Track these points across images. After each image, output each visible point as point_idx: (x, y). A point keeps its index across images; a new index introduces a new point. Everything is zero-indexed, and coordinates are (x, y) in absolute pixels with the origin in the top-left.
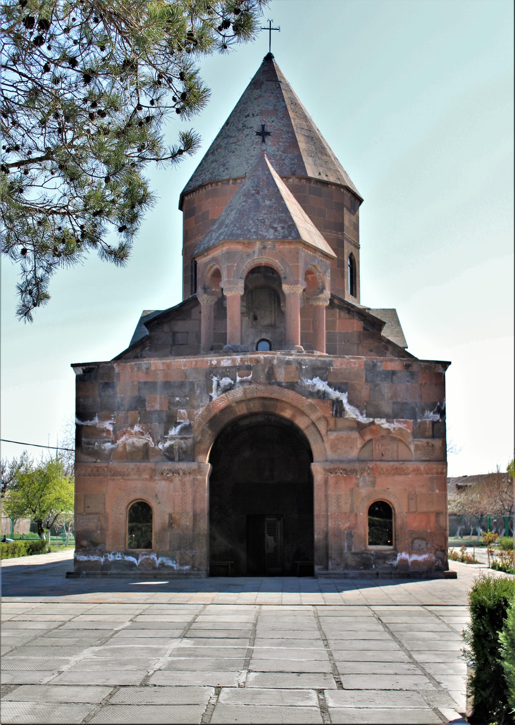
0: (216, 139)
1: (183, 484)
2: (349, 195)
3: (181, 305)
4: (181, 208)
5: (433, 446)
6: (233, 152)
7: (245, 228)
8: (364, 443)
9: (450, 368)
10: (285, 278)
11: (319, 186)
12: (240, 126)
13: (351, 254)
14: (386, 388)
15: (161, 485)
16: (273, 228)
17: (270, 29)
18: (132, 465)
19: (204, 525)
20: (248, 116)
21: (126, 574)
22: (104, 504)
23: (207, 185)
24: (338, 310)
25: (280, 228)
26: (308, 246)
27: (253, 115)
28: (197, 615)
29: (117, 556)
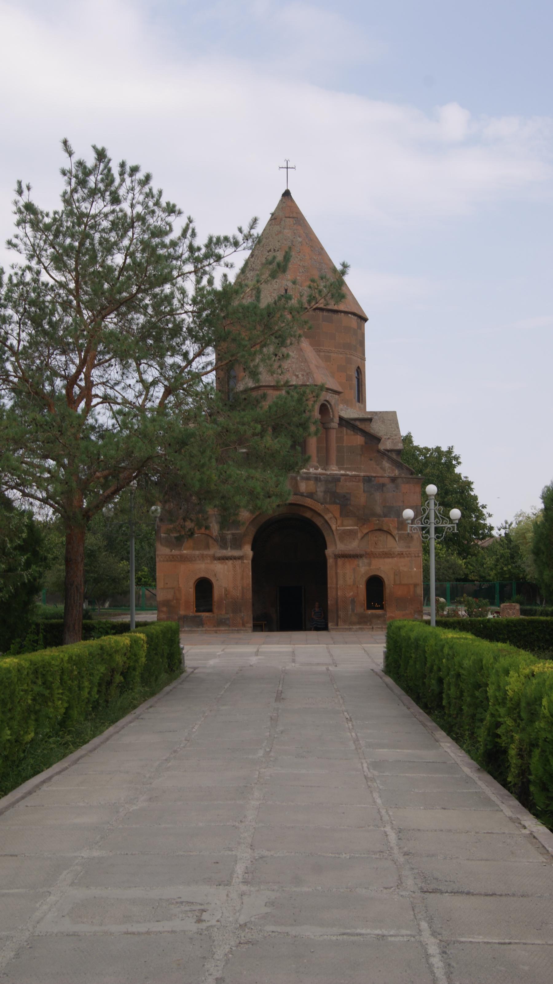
1: (234, 567)
2: (356, 318)
5: (412, 537)
8: (363, 535)
11: (330, 314)
13: (358, 367)
14: (378, 496)
15: (219, 567)
17: (287, 168)
18: (197, 552)
19: (249, 595)
20: (270, 251)
21: (195, 631)
22: (178, 581)
24: (345, 429)
27: (274, 250)
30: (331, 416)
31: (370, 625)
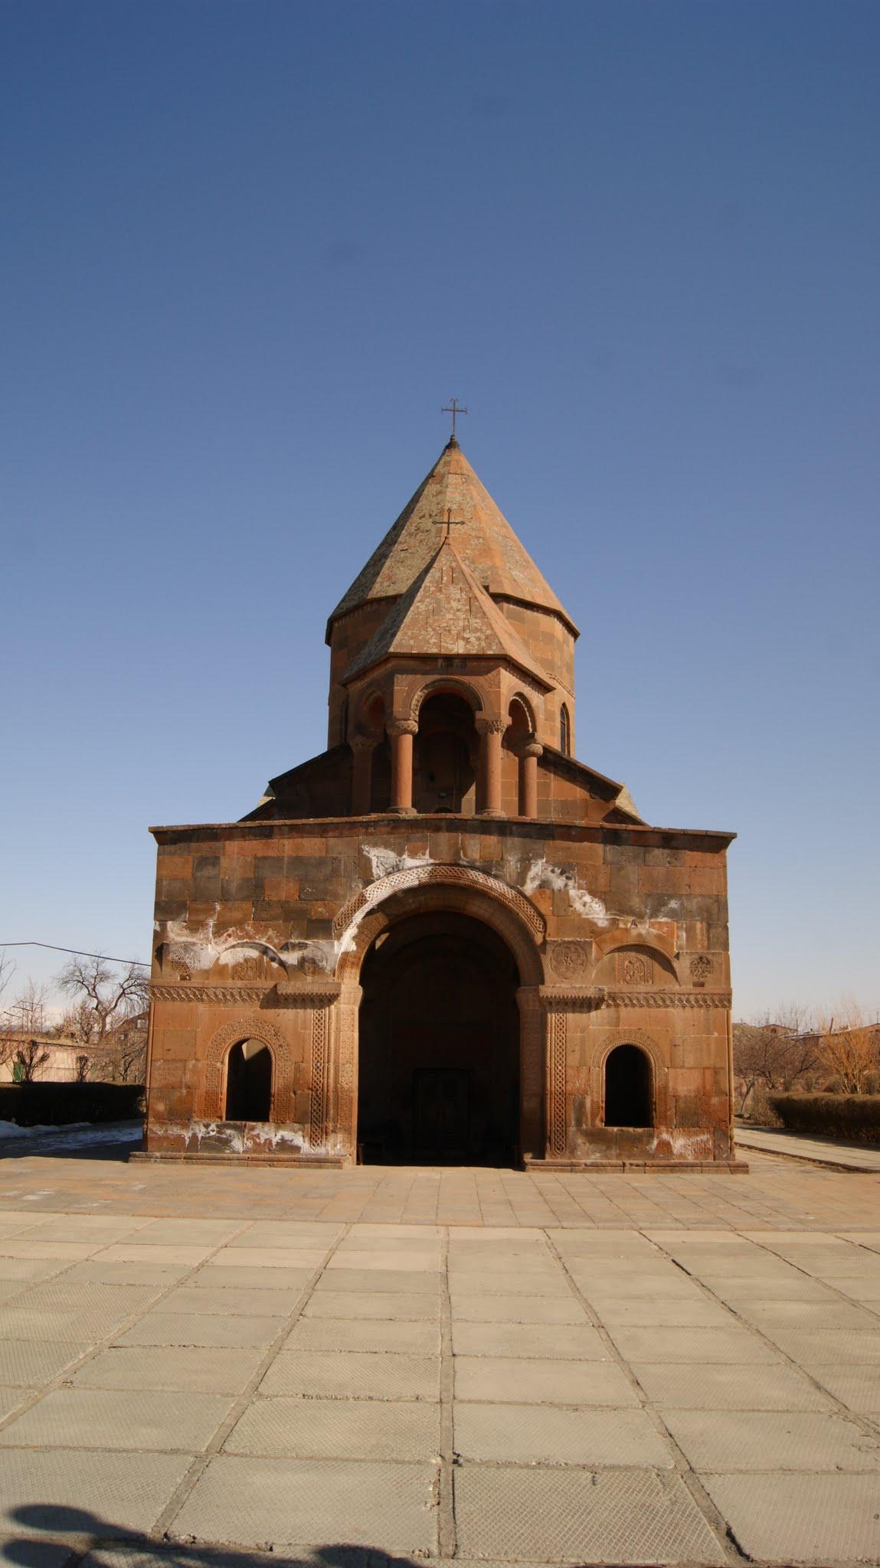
0: (379, 548)
3: (323, 756)
4: (328, 642)
5: (709, 962)
6: (402, 562)
7: (420, 638)
9: (733, 841)
10: (481, 709)
12: (413, 529)
13: (564, 705)
16: (463, 639)
20: (424, 516)
23: (363, 606)
25: (475, 639)
26: (513, 665)
27: (430, 516)
28: (333, 1251)
29: (210, 1128)
30: (531, 730)
31: (619, 1156)
